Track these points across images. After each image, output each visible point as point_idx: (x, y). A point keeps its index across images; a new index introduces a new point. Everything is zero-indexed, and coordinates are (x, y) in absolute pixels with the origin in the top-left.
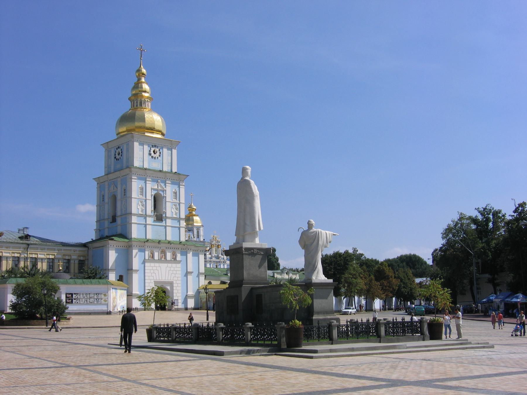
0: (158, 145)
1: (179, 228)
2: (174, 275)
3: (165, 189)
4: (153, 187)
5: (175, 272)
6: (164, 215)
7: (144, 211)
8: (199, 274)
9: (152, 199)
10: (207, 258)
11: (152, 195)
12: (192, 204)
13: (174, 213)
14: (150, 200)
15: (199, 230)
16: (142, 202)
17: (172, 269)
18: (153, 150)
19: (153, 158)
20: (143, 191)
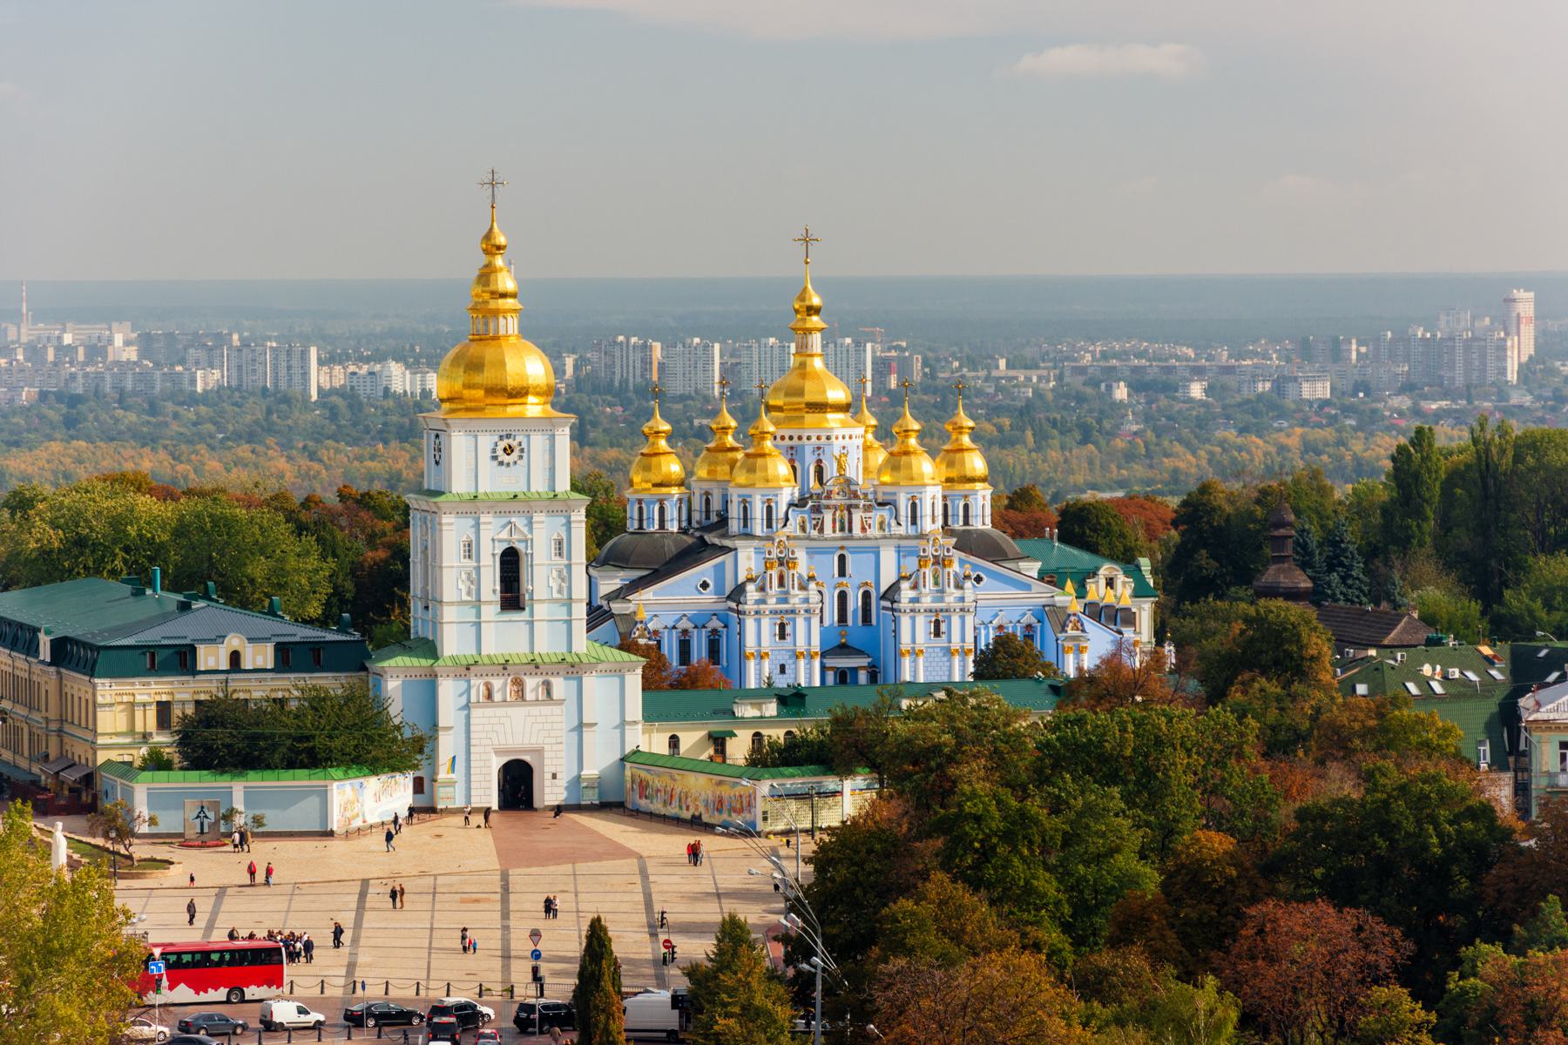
1: (569, 623)
5: (548, 726)
8: (623, 724)
13: (555, 590)
17: (539, 719)
20: (471, 550)
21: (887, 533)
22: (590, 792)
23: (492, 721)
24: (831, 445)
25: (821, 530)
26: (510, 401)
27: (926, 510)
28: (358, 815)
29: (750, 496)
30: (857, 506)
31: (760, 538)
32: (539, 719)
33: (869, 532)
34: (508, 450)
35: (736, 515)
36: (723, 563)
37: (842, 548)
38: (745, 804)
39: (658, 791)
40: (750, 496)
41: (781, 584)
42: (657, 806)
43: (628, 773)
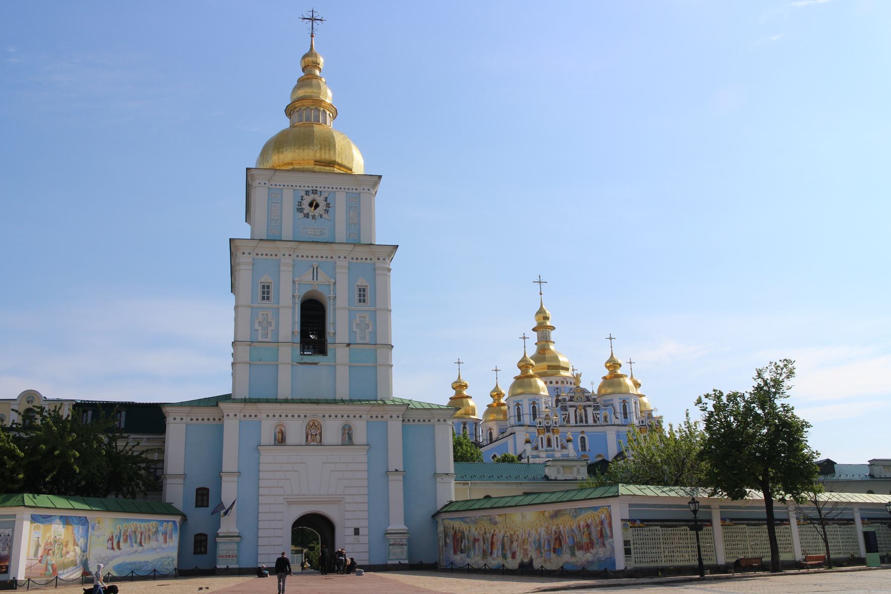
0: (322, 189)
15: (626, 404)
16: (268, 314)
21: (609, 423)
22: (397, 550)
25: (568, 421)
26: (318, 163)
29: (522, 401)
30: (590, 406)
33: (598, 423)
34: (314, 205)
35: (512, 413)
36: (506, 443)
37: (583, 432)
39: (476, 540)
40: (522, 401)
41: (549, 444)
42: (476, 560)
43: (441, 529)
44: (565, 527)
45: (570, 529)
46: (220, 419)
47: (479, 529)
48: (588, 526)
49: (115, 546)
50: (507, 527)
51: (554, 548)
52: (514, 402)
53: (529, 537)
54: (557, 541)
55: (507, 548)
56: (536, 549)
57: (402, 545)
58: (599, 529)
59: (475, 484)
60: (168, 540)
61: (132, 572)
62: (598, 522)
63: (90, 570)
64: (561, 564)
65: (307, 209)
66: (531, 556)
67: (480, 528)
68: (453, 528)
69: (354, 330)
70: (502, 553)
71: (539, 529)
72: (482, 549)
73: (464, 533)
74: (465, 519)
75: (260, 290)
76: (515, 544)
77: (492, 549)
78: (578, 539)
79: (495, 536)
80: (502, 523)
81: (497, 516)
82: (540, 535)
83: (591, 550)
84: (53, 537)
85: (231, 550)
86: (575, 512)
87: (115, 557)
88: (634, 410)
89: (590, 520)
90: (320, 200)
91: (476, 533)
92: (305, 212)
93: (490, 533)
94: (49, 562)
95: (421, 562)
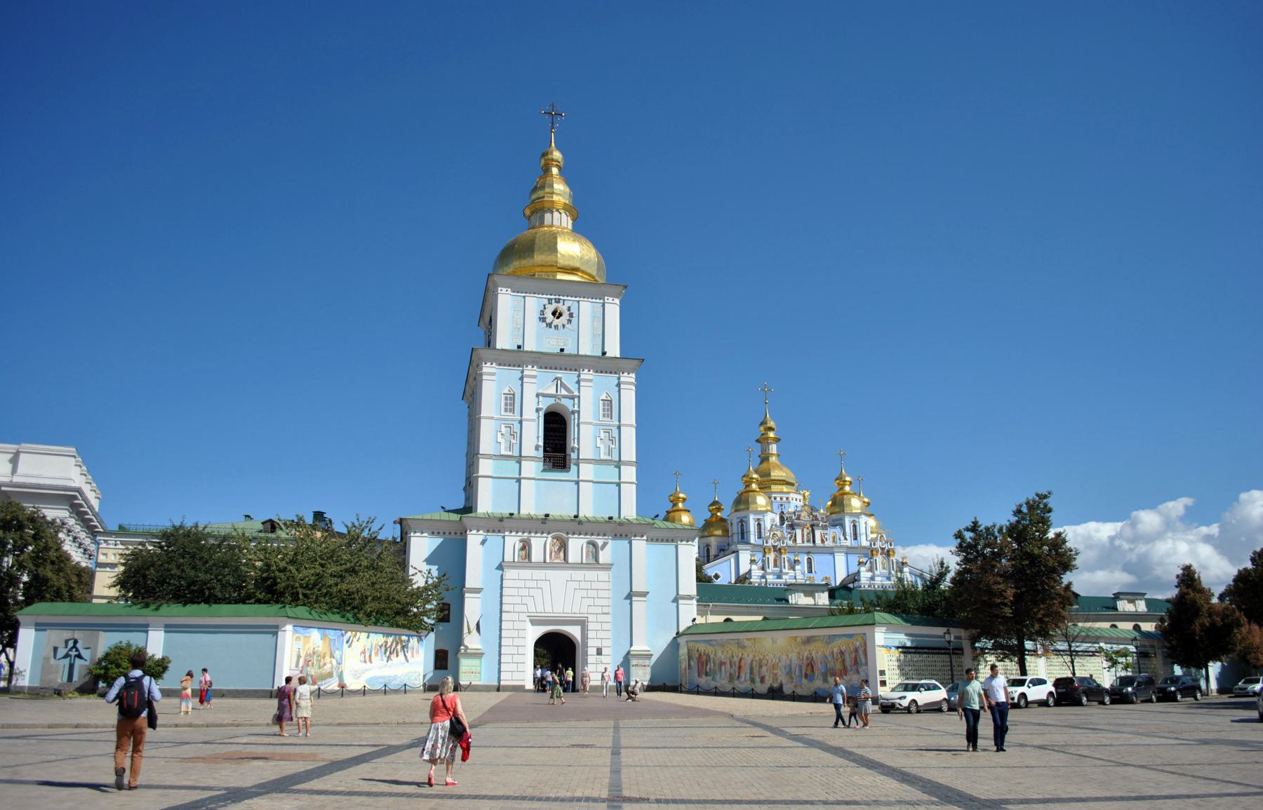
2: (591, 602)
3: (576, 393)
4: (540, 391)
5: (594, 594)
6: (574, 456)
7: (516, 448)
9: (538, 418)
10: (862, 579)
11: (538, 410)
12: (843, 471)
14: (534, 420)
15: (857, 524)
16: (510, 427)
17: (583, 585)
18: (553, 310)
19: (551, 327)
20: (512, 402)
21: (838, 544)
23: (529, 584)
24: (789, 502)
25: (795, 540)
27: (862, 529)
28: (330, 675)
29: (746, 517)
30: (818, 525)
31: (754, 545)
32: (583, 585)
35: (735, 530)
38: (848, 661)
39: (722, 664)
40: (746, 517)
41: (775, 565)
42: (723, 682)
43: (683, 651)
44: (818, 653)
45: (823, 655)
46: (461, 533)
47: (725, 653)
48: (842, 653)
49: (367, 659)
50: (756, 651)
51: (806, 673)
52: (737, 518)
53: (780, 662)
54: (809, 667)
55: (755, 672)
56: (788, 674)
57: (645, 666)
58: (853, 656)
59: (716, 606)
60: (415, 655)
61: (385, 686)
62: (852, 648)
63: (345, 682)
64: (813, 690)
65: (550, 318)
66: (781, 682)
67: (727, 651)
68: (698, 651)
69: (598, 446)
70: (750, 678)
71: (790, 655)
72: (728, 674)
73: (709, 657)
74: (710, 642)
75: (503, 402)
76: (764, 668)
77: (739, 673)
78: (830, 665)
79: (743, 660)
80: (751, 647)
81: (745, 641)
82: (791, 660)
83: (845, 677)
84: (312, 648)
85: (474, 666)
86: (829, 638)
87: (367, 670)
88: (864, 531)
89: (844, 647)
90: (562, 308)
91: (723, 657)
92: (548, 321)
93: (738, 657)
94: (309, 673)
95: (664, 684)
